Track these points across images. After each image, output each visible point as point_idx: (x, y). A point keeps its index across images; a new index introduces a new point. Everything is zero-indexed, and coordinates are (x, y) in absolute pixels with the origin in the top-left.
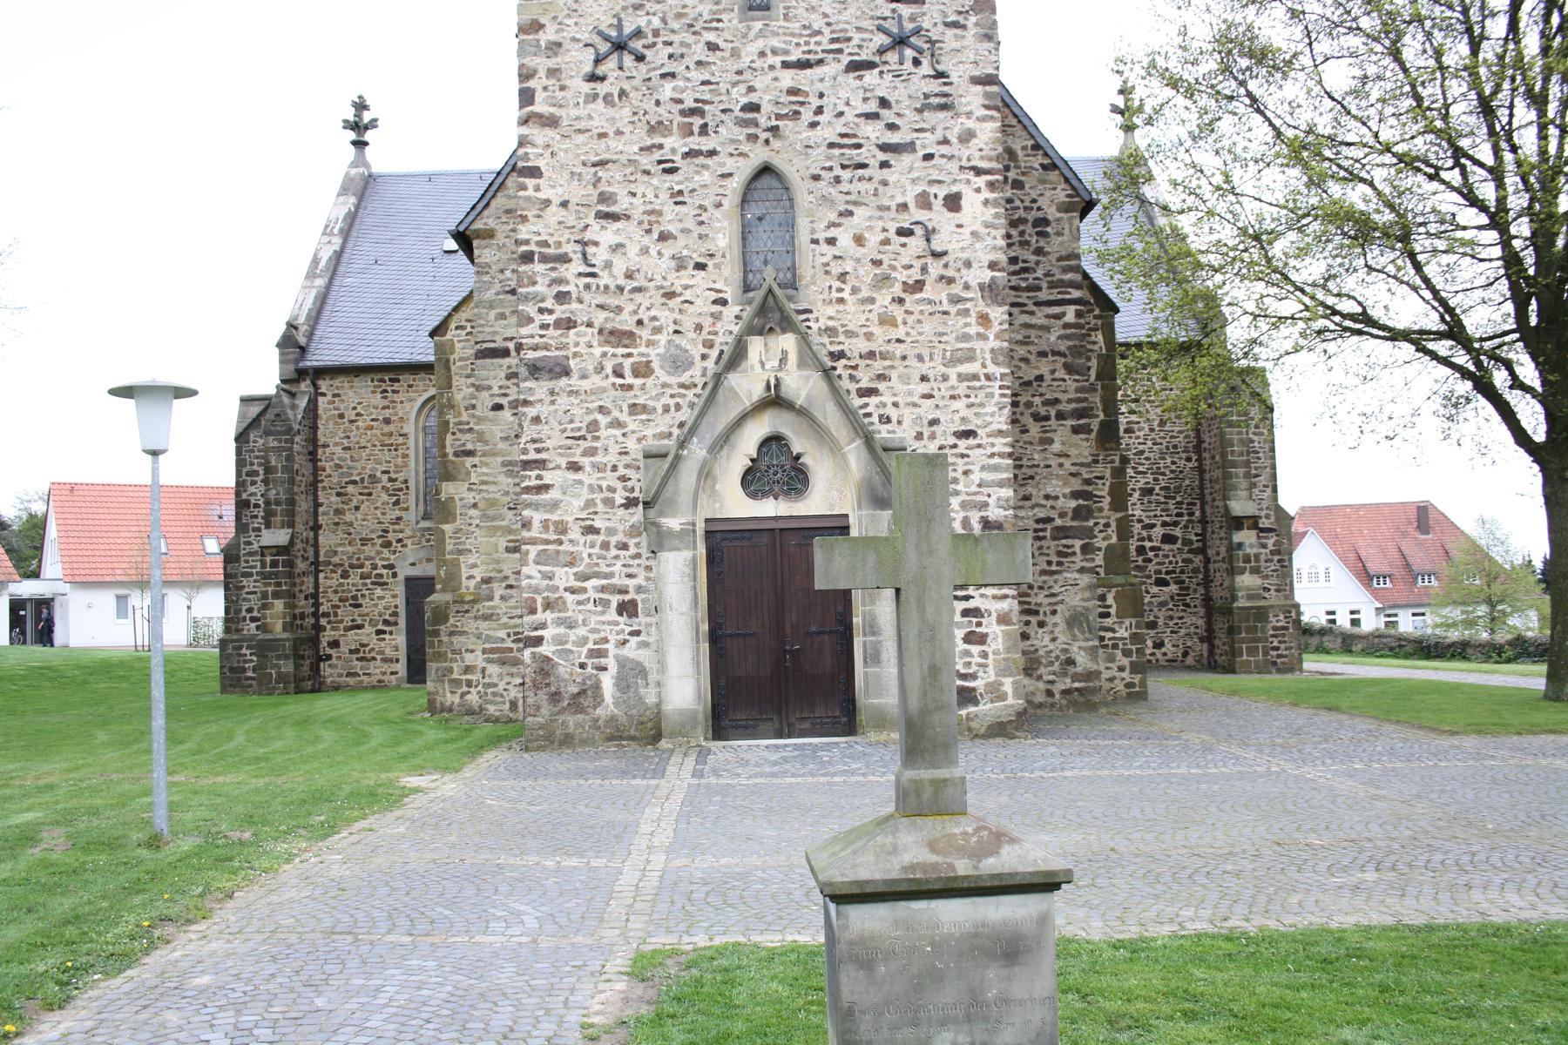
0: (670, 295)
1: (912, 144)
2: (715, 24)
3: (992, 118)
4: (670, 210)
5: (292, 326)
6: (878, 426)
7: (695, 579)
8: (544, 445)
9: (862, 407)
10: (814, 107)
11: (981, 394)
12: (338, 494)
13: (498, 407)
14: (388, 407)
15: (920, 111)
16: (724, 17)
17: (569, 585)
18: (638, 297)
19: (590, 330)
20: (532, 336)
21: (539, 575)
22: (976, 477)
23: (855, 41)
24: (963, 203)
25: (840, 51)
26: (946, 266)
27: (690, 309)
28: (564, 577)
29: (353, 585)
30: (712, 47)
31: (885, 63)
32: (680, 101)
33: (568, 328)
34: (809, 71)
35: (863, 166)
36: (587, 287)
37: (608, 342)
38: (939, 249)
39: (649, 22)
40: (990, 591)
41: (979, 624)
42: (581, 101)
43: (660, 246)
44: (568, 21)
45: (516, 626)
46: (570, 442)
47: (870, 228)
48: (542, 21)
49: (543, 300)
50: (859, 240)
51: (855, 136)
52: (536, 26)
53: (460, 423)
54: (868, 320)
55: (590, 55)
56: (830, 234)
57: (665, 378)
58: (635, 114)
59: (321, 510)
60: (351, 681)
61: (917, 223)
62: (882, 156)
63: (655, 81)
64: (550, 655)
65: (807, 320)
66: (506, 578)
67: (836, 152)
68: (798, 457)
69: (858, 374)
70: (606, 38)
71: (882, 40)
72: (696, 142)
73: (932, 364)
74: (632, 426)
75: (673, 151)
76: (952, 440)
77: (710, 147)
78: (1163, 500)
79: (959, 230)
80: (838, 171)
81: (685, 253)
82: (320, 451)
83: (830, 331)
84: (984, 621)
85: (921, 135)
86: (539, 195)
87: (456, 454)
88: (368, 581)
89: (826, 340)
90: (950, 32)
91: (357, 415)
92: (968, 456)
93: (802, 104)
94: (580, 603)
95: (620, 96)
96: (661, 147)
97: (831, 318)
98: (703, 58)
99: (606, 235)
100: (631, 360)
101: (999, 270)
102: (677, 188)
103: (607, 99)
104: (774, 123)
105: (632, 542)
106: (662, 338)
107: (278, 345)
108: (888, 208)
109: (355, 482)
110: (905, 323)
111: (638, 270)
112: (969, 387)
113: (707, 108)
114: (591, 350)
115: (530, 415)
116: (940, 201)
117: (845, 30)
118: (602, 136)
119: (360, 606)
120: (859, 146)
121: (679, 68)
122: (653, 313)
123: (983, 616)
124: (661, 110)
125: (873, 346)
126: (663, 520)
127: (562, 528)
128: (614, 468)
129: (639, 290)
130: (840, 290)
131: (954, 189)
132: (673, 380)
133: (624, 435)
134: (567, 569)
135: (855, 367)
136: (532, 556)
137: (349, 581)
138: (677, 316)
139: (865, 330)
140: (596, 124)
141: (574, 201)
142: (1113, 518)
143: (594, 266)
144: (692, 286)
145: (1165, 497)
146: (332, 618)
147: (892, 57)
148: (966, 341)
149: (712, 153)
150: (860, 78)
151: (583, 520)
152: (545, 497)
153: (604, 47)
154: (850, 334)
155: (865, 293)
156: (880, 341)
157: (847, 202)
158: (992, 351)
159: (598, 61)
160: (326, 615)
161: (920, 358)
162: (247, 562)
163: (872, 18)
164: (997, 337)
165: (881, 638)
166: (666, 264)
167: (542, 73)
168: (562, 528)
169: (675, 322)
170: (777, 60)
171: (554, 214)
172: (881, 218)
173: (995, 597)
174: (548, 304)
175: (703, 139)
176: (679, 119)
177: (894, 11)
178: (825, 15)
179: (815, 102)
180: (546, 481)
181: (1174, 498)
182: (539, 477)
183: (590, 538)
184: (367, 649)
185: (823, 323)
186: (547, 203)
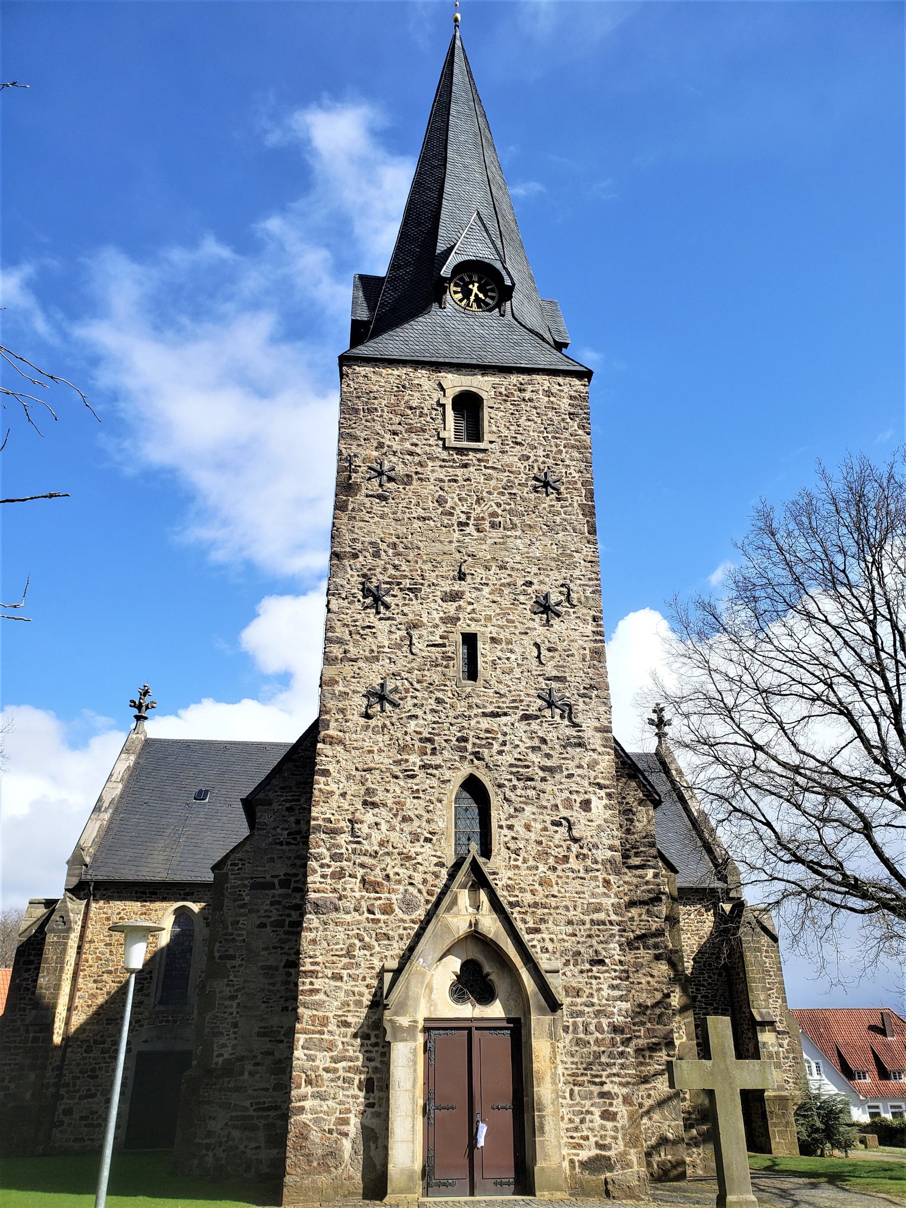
0: (409, 858)
1: (560, 767)
2: (442, 687)
3: (609, 754)
4: (409, 802)
5: (79, 848)
6: (540, 955)
7: (415, 1063)
8: (317, 960)
9: (529, 941)
10: (500, 740)
11: (607, 934)
12: (95, 981)
13: (262, 925)
14: (145, 914)
17: (327, 1065)
18: (388, 859)
19: (354, 880)
21: (305, 1058)
22: (605, 993)
24: (593, 806)
25: (517, 708)
26: (581, 848)
27: (420, 868)
28: (323, 1060)
29: (94, 1059)
30: (439, 701)
31: (545, 716)
32: (420, 733)
33: (340, 878)
35: (532, 780)
36: (354, 851)
38: (576, 833)
39: (403, 684)
40: (616, 1079)
41: (611, 1104)
43: (404, 825)
45: (257, 1097)
46: (335, 958)
47: (535, 820)
50: (528, 827)
51: (526, 760)
52: (333, 682)
53: (226, 934)
54: (533, 881)
56: (509, 823)
57: (401, 915)
58: (391, 739)
59: (78, 994)
60: (77, 1146)
61: (564, 818)
62: (541, 774)
63: (405, 720)
64: (308, 1122)
65: (495, 879)
66: (255, 1057)
67: (514, 770)
68: (488, 974)
69: (528, 918)
72: (428, 759)
73: (575, 913)
74: (377, 949)
75: (414, 764)
76: (588, 966)
77: (438, 762)
78: (704, 1006)
79: (590, 824)
80: (515, 782)
81: (419, 830)
82: (87, 946)
83: (508, 887)
84: (615, 1102)
85: (567, 762)
86: (327, 788)
87: (220, 958)
88: (106, 1055)
89: (505, 893)
90: (581, 700)
91: (121, 918)
92: (600, 978)
93: (494, 739)
94: (332, 1080)
96: (407, 761)
97: (509, 878)
98: (434, 707)
99: (369, 817)
100: (379, 902)
101: (616, 851)
102: (415, 788)
104: (477, 750)
105: (373, 1034)
106: (401, 888)
107: (68, 863)
108: (546, 808)
109: (110, 972)
110: (557, 884)
111: (388, 841)
112: (599, 930)
113: (436, 738)
114: (354, 894)
115: (309, 938)
116: (578, 805)
117: (520, 695)
118: (370, 752)
119: (97, 1077)
120: (528, 767)
121: (420, 713)
122: (396, 870)
123: (613, 1099)
124: (408, 738)
125: (537, 899)
126: (397, 1018)
127: (324, 1021)
128: (364, 979)
129: (388, 854)
130: (516, 860)
131: (587, 797)
132: (406, 917)
133: (371, 955)
134: (325, 1053)
135: (525, 913)
136: (301, 1043)
137: (92, 1055)
138: (411, 872)
139: (532, 887)
140: (366, 744)
141: (349, 792)
142: (682, 1023)
143: (359, 837)
144: (421, 853)
145: (706, 1004)
146: (71, 1088)
148: (596, 898)
149: (437, 767)
150: (529, 724)
151: (340, 1016)
152: (316, 998)
154: (522, 890)
155: (531, 863)
156: (541, 896)
157: (521, 802)
158: (613, 904)
160: (67, 1085)
161: (567, 908)
162: (8, 1037)
163: (536, 689)
164: (616, 895)
165: (544, 1113)
166: (406, 837)
168: (324, 1021)
169: (410, 877)
170: (480, 711)
171: (334, 801)
172: (542, 814)
173: (621, 1084)
174: (327, 861)
175: (434, 757)
176: (417, 744)
179: (501, 738)
180: (316, 986)
181: (711, 1005)
182: (312, 983)
183: (343, 1029)
184: (95, 1117)
185: (505, 881)
186: (332, 793)
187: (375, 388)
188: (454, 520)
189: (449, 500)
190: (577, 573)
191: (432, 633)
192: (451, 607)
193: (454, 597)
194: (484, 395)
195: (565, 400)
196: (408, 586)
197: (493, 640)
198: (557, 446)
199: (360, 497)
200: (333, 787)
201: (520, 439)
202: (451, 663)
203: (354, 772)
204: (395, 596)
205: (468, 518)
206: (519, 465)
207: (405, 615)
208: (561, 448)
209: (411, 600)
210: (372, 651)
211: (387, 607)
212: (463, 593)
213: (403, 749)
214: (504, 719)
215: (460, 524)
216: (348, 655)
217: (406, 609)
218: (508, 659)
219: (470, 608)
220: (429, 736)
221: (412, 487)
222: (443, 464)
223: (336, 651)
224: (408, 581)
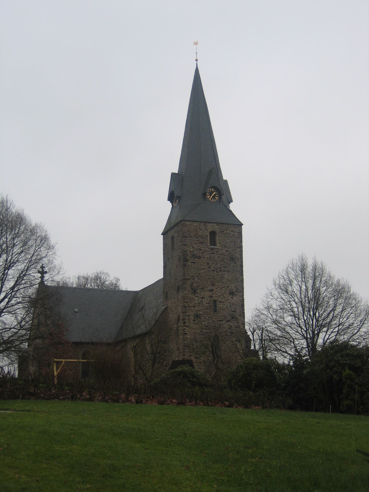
2: (210, 314)
15: (235, 328)
16: (211, 313)
20: (186, 357)
23: (227, 317)
30: (209, 317)
31: (231, 321)
32: (205, 325)
34: (222, 322)
37: (196, 359)
39: (201, 313)
42: (192, 324)
44: (190, 312)
48: (187, 312)
49: (187, 352)
55: (193, 317)
70: (196, 315)
71: (230, 317)
90: (239, 316)
95: (197, 324)
98: (208, 319)
100: (199, 361)
103: (196, 324)
117: (226, 316)
118: (195, 329)
147: (232, 320)
153: (195, 316)
159: (195, 318)
167: (187, 319)
170: (217, 320)
177: (232, 313)
178: (224, 313)
186: (188, 338)
187: (191, 230)
188: (211, 269)
189: (207, 262)
190: (239, 284)
191: (207, 300)
192: (211, 293)
193: (211, 290)
194: (217, 232)
195: (237, 233)
196: (201, 288)
197: (221, 302)
198: (235, 247)
199: (189, 263)
200: (188, 337)
201: (226, 245)
202: (212, 308)
203: (192, 334)
204: (198, 290)
205: (214, 269)
206: (226, 253)
207: (201, 295)
208: (236, 248)
209: (202, 291)
210: (194, 305)
211: (197, 293)
212: (213, 289)
213: (202, 329)
214: (222, 322)
215: (213, 270)
216: (189, 306)
217: (201, 294)
218: (224, 307)
219: (215, 293)
220: (207, 326)
221: (201, 260)
222: (208, 253)
223: (186, 304)
224: (201, 286)
